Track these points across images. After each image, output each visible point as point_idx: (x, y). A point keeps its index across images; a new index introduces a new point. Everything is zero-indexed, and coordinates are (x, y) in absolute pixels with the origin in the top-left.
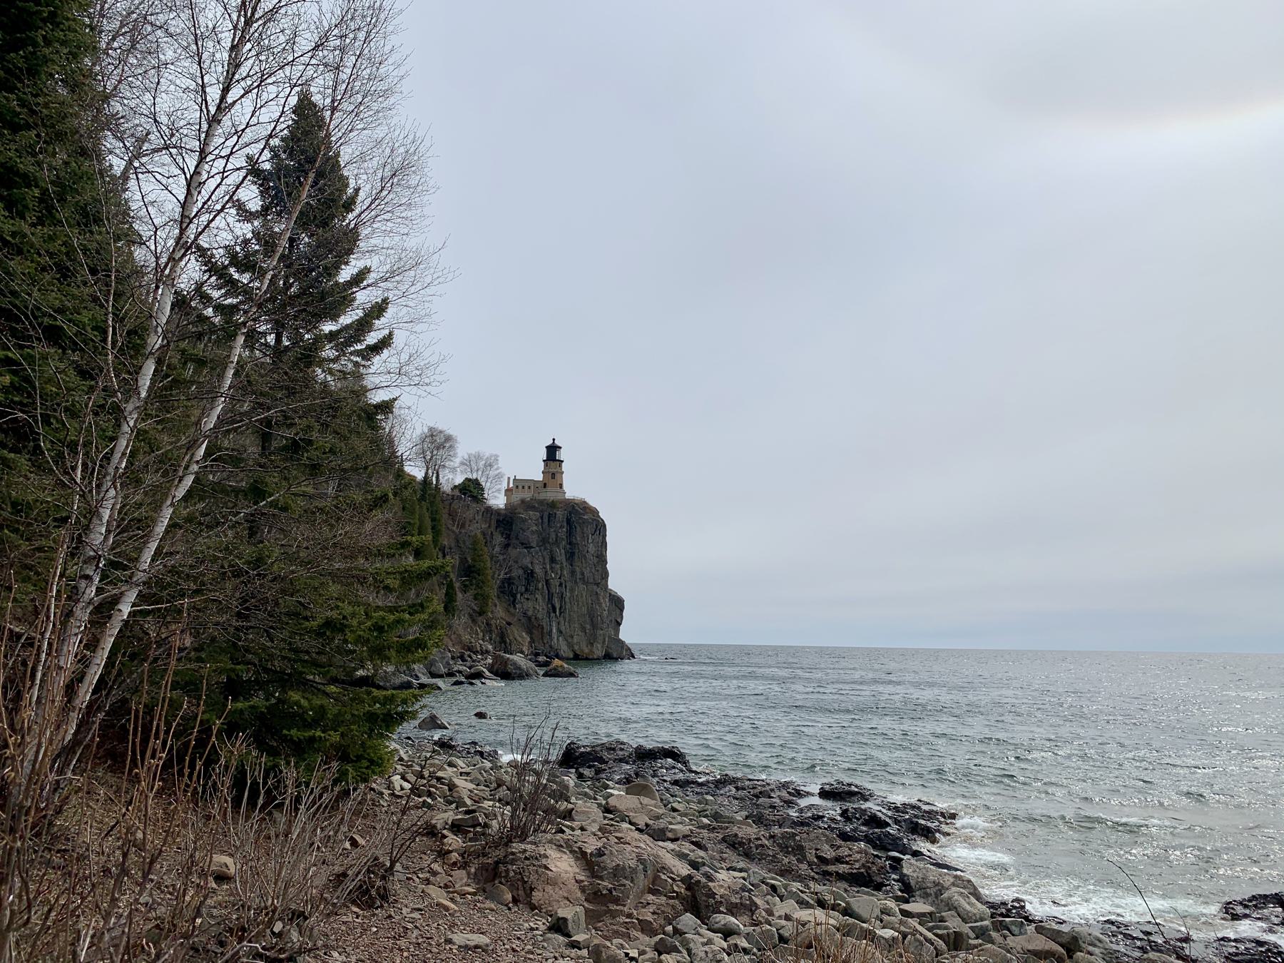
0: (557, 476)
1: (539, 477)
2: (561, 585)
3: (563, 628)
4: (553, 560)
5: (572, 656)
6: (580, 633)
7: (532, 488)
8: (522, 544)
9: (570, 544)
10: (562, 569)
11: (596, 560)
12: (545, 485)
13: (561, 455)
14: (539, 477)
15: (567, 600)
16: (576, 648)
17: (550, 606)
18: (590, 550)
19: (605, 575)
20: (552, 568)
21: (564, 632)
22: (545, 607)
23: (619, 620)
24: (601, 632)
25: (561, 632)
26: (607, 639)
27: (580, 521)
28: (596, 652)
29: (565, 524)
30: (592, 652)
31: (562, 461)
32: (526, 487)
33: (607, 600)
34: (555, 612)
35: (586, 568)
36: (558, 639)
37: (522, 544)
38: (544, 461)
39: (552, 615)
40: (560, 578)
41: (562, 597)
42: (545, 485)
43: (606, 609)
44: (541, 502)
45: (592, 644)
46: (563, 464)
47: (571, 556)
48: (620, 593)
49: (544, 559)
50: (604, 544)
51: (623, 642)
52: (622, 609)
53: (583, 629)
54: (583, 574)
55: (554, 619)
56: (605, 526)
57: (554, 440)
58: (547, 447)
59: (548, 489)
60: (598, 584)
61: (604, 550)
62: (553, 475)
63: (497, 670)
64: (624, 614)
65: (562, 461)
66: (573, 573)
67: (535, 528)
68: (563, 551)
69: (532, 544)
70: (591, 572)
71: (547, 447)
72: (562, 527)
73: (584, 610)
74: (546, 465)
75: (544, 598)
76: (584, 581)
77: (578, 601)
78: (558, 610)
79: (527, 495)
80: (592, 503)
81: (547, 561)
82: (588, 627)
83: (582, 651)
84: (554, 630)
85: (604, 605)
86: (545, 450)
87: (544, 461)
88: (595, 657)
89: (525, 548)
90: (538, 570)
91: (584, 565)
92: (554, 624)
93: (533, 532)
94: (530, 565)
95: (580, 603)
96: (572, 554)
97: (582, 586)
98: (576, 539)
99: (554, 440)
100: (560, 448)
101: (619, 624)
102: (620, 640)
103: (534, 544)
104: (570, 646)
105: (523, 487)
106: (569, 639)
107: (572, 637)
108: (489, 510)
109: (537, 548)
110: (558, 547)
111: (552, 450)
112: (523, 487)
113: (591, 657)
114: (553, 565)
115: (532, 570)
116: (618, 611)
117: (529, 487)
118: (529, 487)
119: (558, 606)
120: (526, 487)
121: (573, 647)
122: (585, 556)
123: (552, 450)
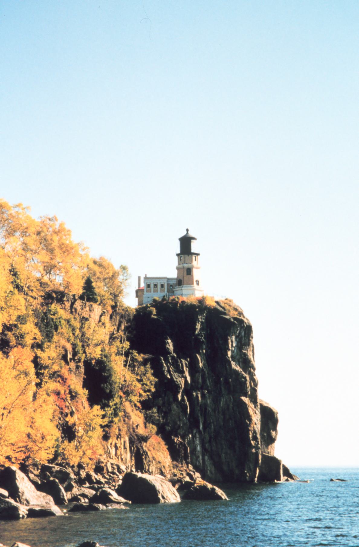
14: (173, 274)
16: (225, 468)
31: (198, 254)
32: (159, 286)
38: (178, 255)
57: (187, 230)
74: (180, 260)
87: (178, 255)
99: (187, 230)
100: (194, 239)
105: (156, 285)
118: (162, 286)
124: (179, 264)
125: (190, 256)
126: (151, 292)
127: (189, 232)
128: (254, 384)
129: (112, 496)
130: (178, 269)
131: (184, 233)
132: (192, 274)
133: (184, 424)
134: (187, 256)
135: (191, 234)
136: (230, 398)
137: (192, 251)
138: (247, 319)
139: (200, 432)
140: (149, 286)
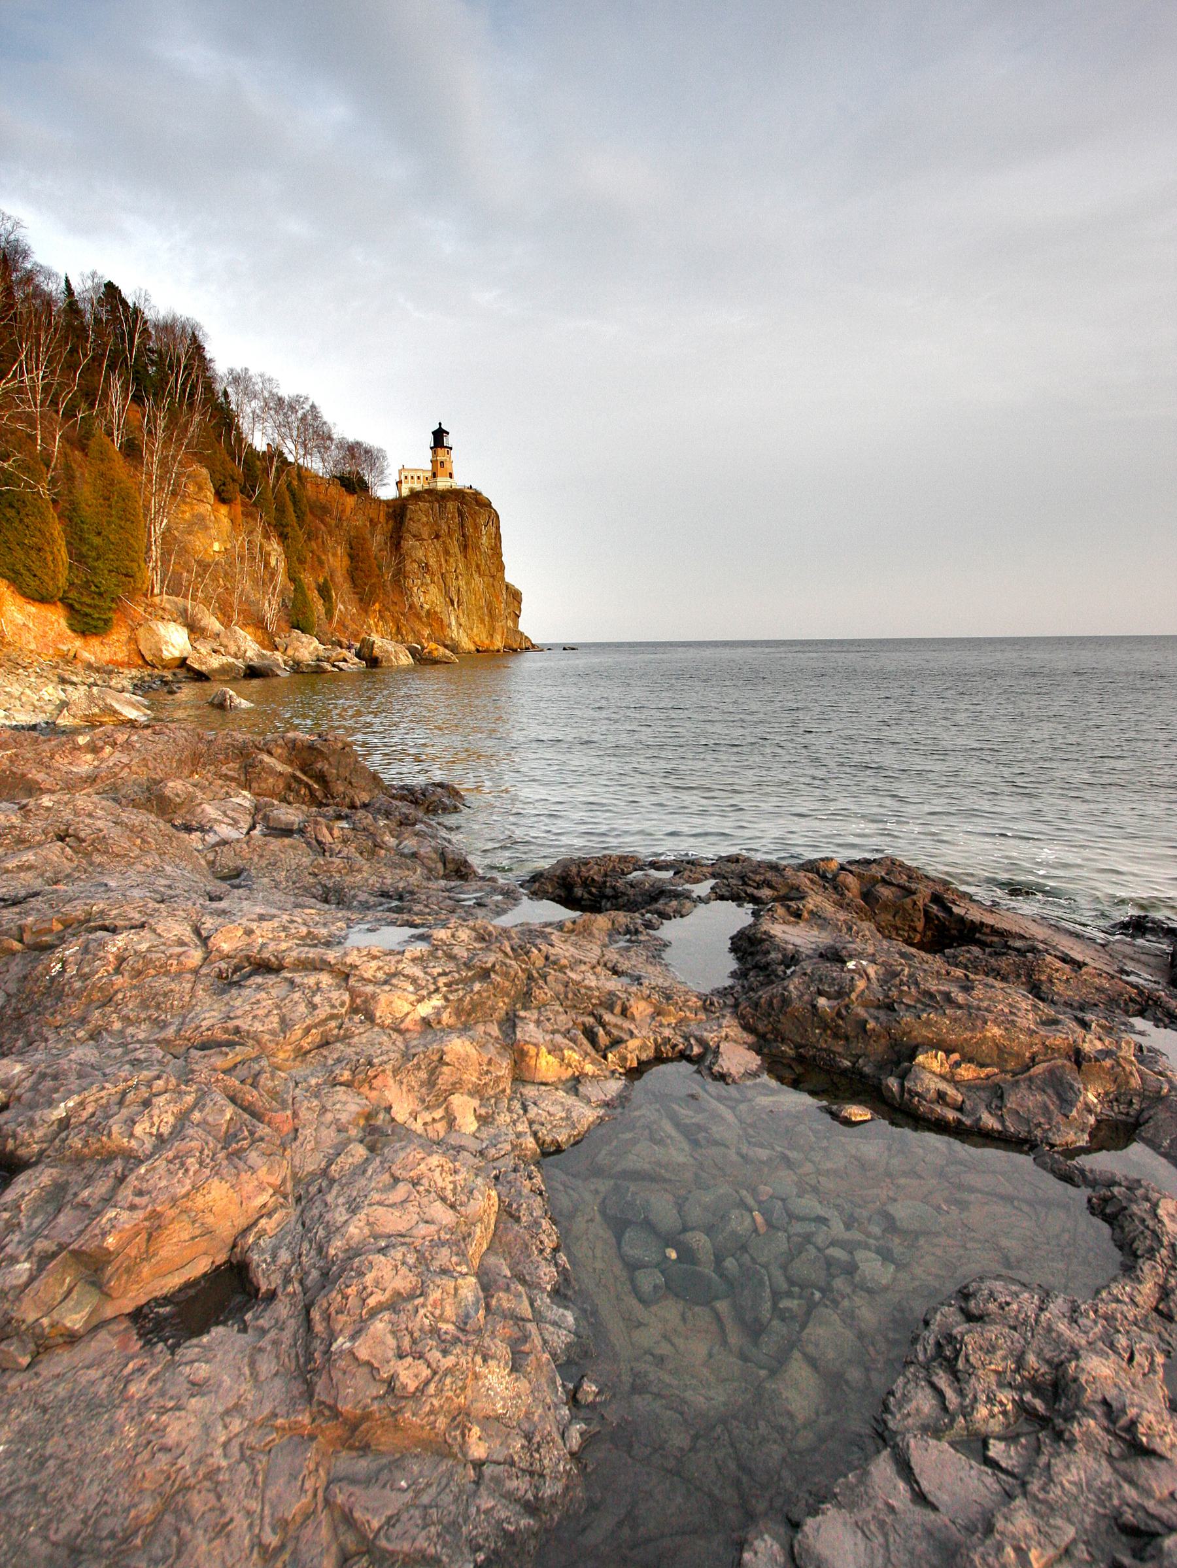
1: (429, 467)
3: (463, 621)
5: (473, 648)
8: (414, 536)
9: (463, 536)
11: (490, 552)
12: (434, 475)
13: (448, 441)
16: (477, 639)
19: (501, 567)
20: (446, 561)
34: (453, 605)
39: (451, 608)
44: (430, 492)
45: (492, 636)
47: (464, 547)
48: (518, 586)
52: (520, 603)
53: (482, 621)
54: (478, 566)
59: (439, 479)
60: (493, 577)
66: (468, 567)
73: (482, 603)
74: (435, 453)
80: (486, 494)
81: (441, 554)
82: (487, 619)
84: (454, 623)
92: (453, 618)
93: (424, 525)
103: (425, 536)
106: (468, 631)
108: (378, 501)
111: (439, 435)
116: (516, 604)
123: (439, 435)
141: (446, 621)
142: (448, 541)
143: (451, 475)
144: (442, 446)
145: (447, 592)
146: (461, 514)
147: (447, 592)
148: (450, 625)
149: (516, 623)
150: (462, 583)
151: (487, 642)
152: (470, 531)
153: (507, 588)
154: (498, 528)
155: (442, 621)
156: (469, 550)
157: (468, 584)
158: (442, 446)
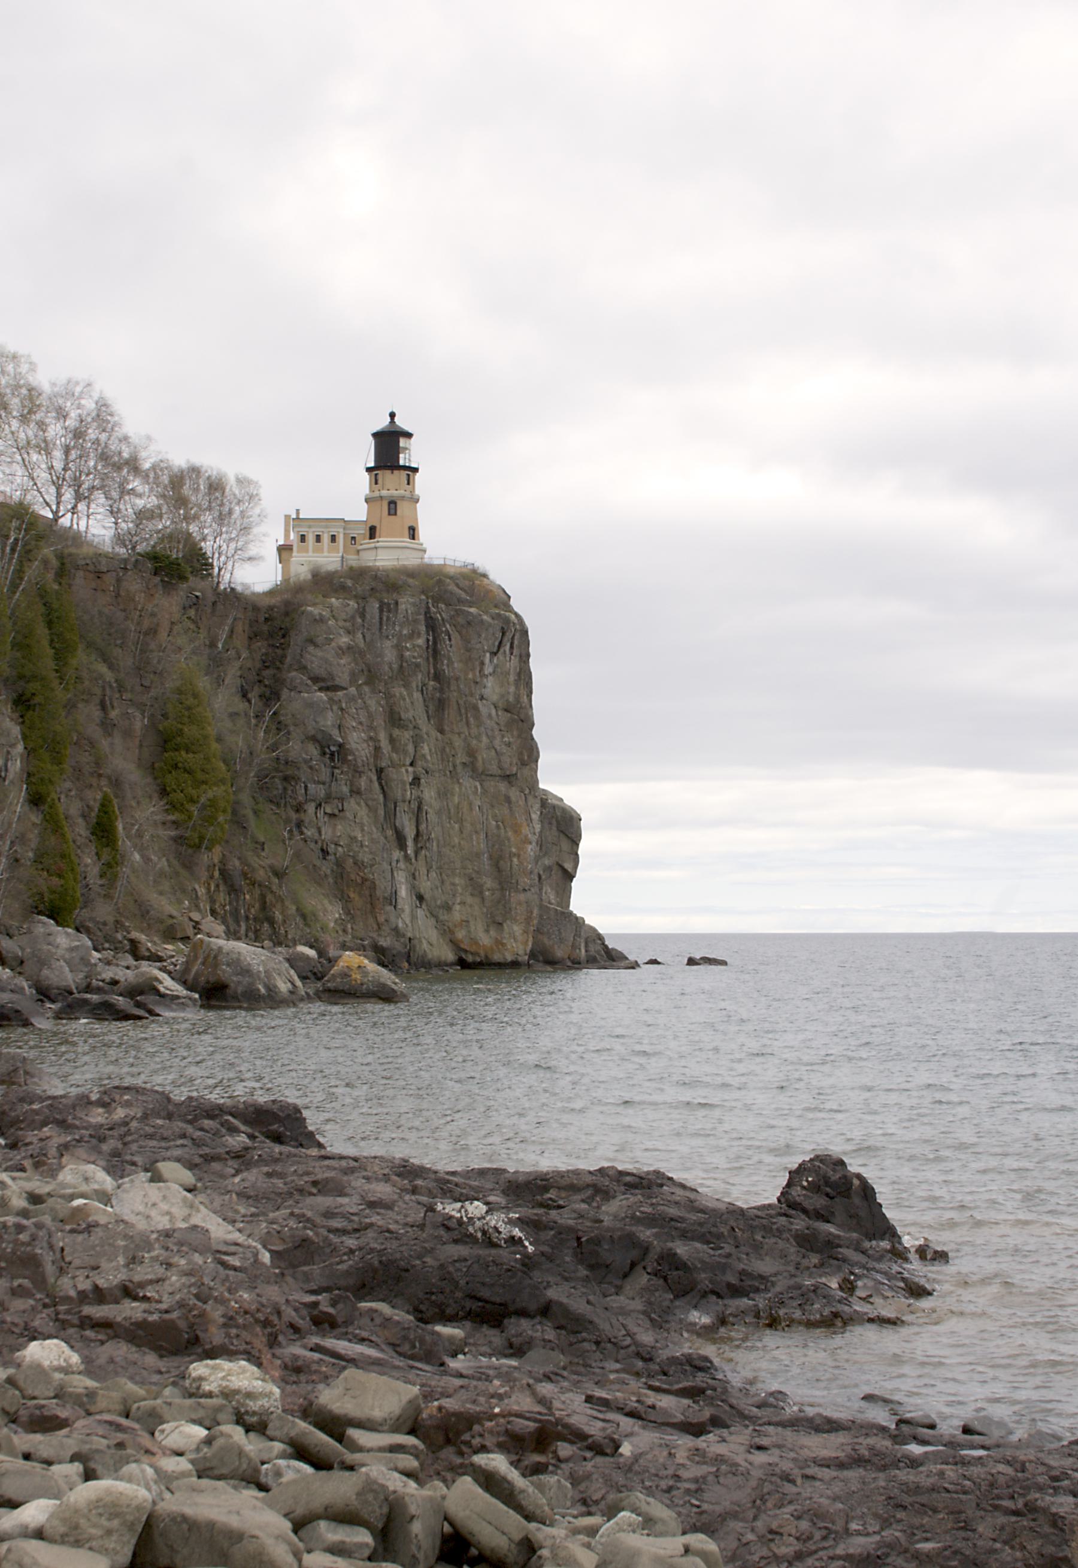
0: (402, 508)
1: (359, 512)
2: (416, 781)
3: (425, 886)
4: (394, 719)
5: (450, 956)
6: (469, 900)
7: (340, 539)
8: (316, 679)
9: (438, 677)
10: (417, 741)
11: (504, 717)
12: (372, 532)
13: (412, 453)
14: (359, 512)
15: (432, 816)
16: (460, 934)
17: (389, 833)
18: (487, 692)
19: (529, 754)
20: (392, 740)
21: (427, 896)
22: (376, 834)
23: (568, 866)
24: (522, 897)
25: (420, 898)
26: (536, 912)
27: (461, 620)
28: (511, 944)
29: (423, 628)
30: (499, 943)
31: (416, 470)
32: (326, 539)
33: (535, 816)
35: (478, 738)
36: (414, 917)
37: (316, 679)
38: (369, 470)
39: (397, 854)
40: (411, 764)
41: (419, 813)
42: (372, 532)
43: (534, 839)
44: (359, 574)
46: (418, 476)
47: (438, 707)
49: (370, 716)
50: (524, 678)
51: (578, 922)
52: (574, 839)
53: (477, 890)
54: (471, 753)
55: (402, 865)
56: (525, 633)
57: (392, 415)
58: (379, 437)
59: (382, 540)
60: (509, 778)
61: (523, 691)
62: (393, 506)
63: (195, 978)
64: (583, 848)
65: (416, 470)
67: (344, 640)
68: (417, 695)
69: (338, 682)
70: (491, 747)
71: (379, 437)
72: (413, 635)
73: (480, 843)
75: (373, 810)
76: (474, 769)
77: (461, 821)
78: (410, 843)
79: (330, 559)
81: (380, 721)
82: (489, 883)
83: (474, 941)
84: (403, 892)
85: (525, 830)
86: (371, 442)
87: (369, 470)
88: (509, 958)
89: (320, 689)
90: (357, 742)
91: (474, 731)
92: (401, 877)
93: (342, 651)
94: (335, 733)
95: (468, 826)
96: (441, 705)
97: (468, 783)
98: (450, 663)
99: (392, 415)
100: (409, 435)
101: (569, 876)
102: (571, 913)
103: (343, 678)
104: (447, 932)
105: (318, 539)
106: (438, 912)
107: (448, 908)
108: (233, 597)
109: (353, 690)
110: (406, 686)
112: (318, 539)
113: (497, 957)
114: (396, 732)
115: (340, 746)
116: (565, 845)
117: (333, 538)
118: (333, 538)
119: (410, 832)
120: (326, 539)
121: (452, 932)
122: (476, 708)
124: (372, 490)
125: (396, 472)
126: (307, 551)
127: (396, 419)
128: (529, 757)
129: (161, 983)
130: (367, 500)
131: (383, 423)
132: (399, 512)
133: (372, 840)
134: (389, 472)
135: (401, 422)
136: (476, 787)
137: (401, 463)
138: (517, 615)
139: (407, 857)
140: (303, 538)
141: (383, 887)
142: (398, 690)
143: (413, 532)
144: (395, 466)
145: (391, 815)
146: (432, 625)
147: (391, 815)
148: (392, 899)
149: (565, 893)
150: (429, 794)
151: (485, 940)
152: (454, 663)
153: (544, 803)
154: (525, 657)
155: (373, 887)
156: (451, 713)
157: (443, 794)
158: (395, 466)
